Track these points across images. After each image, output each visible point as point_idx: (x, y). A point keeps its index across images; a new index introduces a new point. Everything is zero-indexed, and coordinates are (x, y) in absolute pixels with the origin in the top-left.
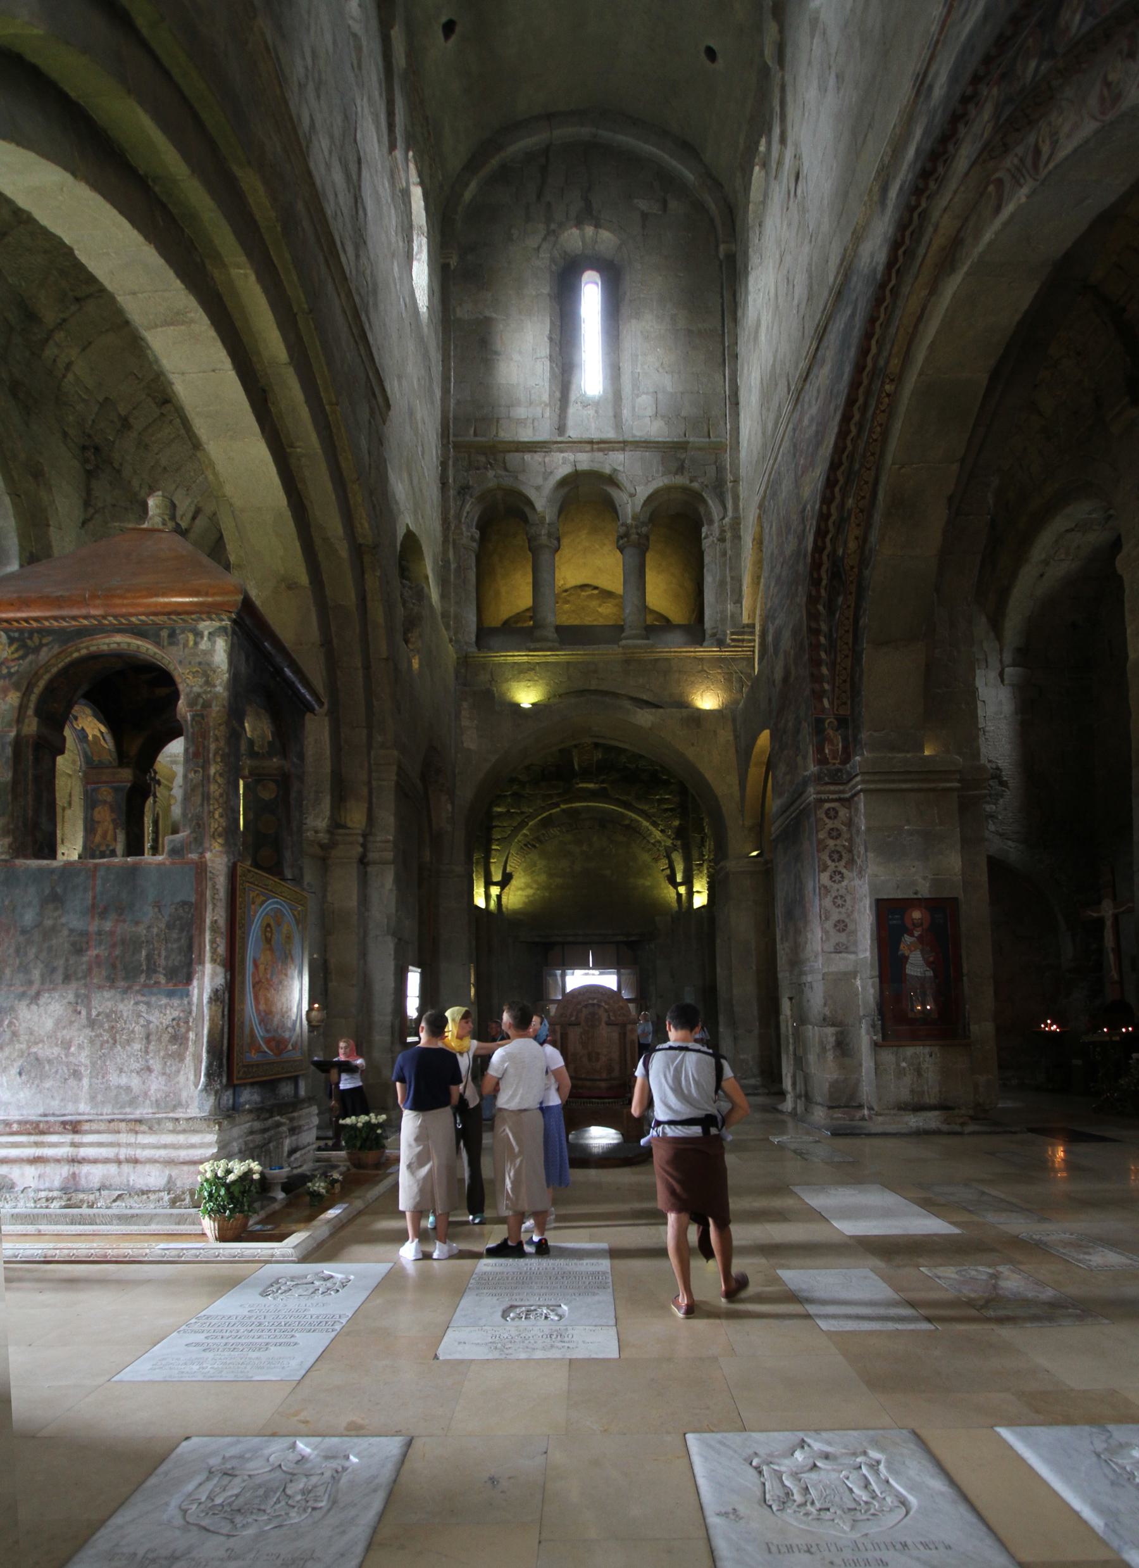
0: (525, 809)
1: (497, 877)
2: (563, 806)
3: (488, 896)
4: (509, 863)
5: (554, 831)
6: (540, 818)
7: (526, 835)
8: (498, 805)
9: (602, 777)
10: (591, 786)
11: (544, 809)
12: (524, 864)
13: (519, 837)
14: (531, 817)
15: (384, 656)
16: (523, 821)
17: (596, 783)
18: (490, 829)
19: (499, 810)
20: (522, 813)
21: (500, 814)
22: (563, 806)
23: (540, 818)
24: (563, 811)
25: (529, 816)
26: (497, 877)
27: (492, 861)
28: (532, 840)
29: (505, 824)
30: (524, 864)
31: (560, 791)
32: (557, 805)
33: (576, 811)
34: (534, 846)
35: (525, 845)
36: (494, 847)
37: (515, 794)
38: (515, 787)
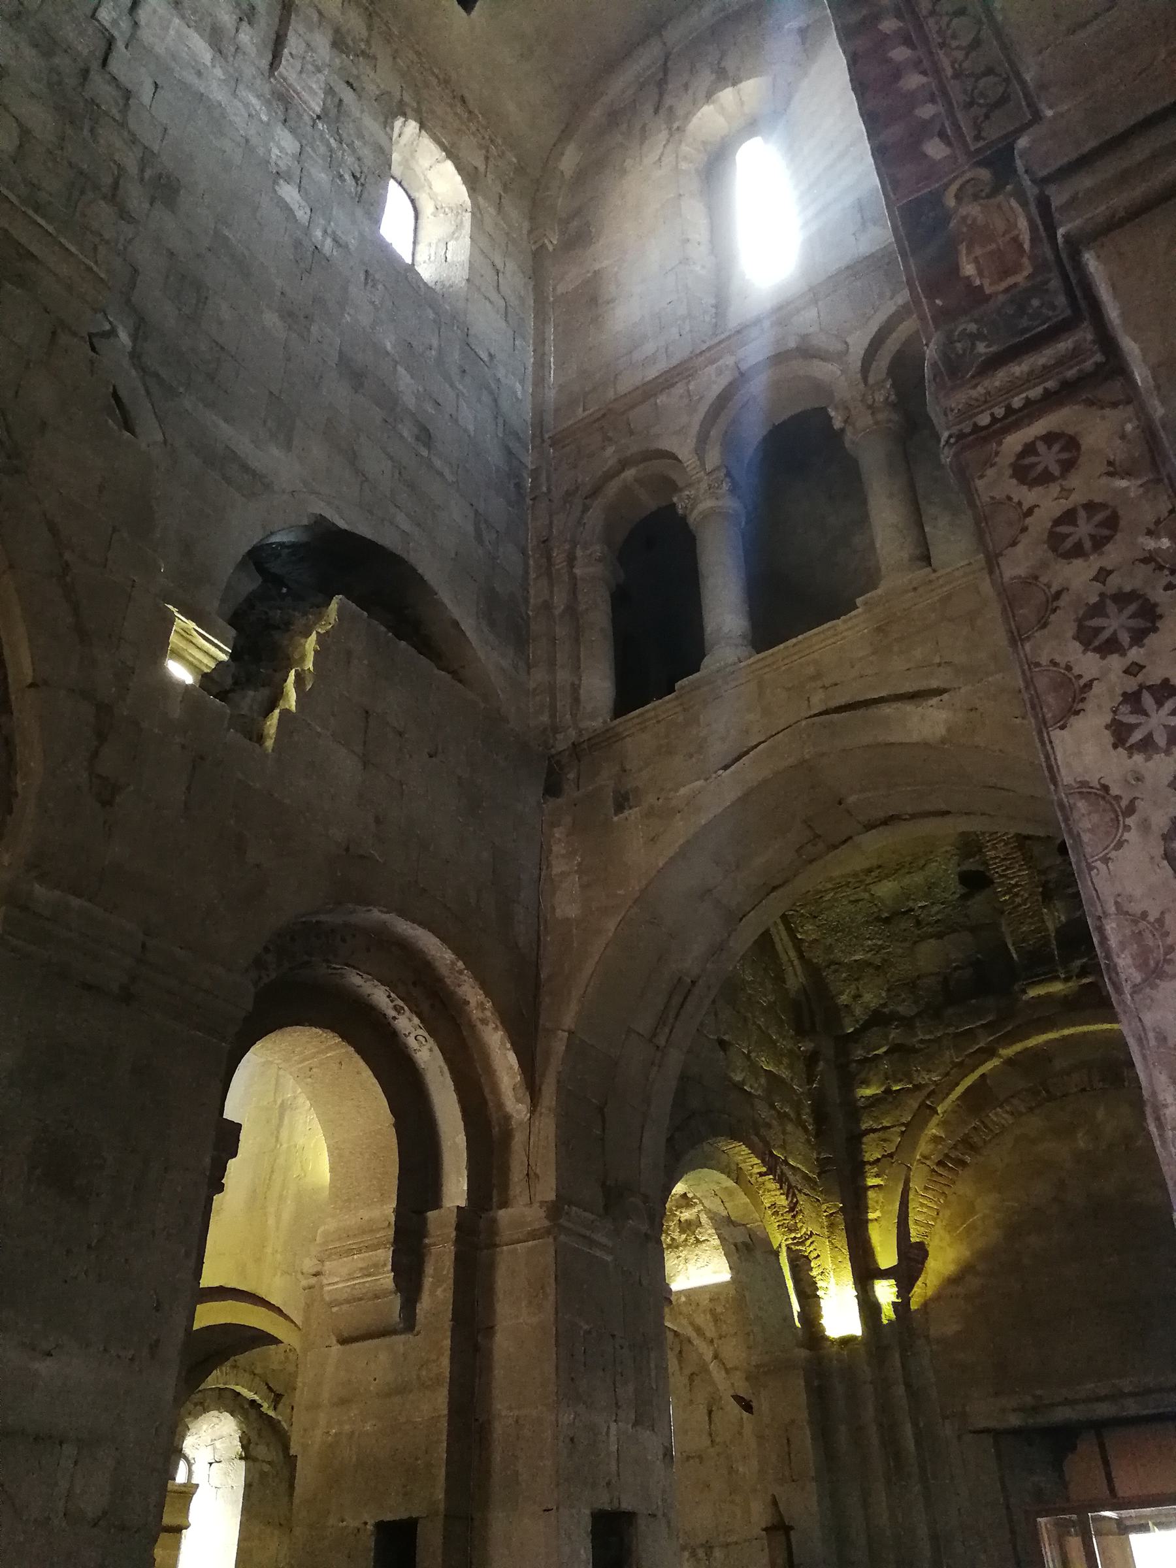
0: (923, 1078)
1: (886, 1256)
2: (1008, 1052)
3: (868, 1307)
4: (912, 1216)
5: (999, 1116)
6: (960, 1090)
7: (936, 1139)
8: (866, 1083)
9: (1079, 963)
10: (1057, 987)
11: (965, 1068)
12: (947, 1213)
13: (923, 1147)
14: (939, 1092)
15: (29, 680)
16: (923, 1105)
17: (1067, 980)
18: (855, 1140)
19: (868, 1092)
20: (918, 1087)
21: (874, 1101)
22: (1008, 1052)
23: (960, 1090)
24: (1010, 1062)
25: (929, 1096)
26: (886, 1256)
27: (871, 1216)
28: (955, 1147)
29: (886, 1123)
30: (947, 1213)
31: (991, 1018)
32: (990, 1052)
33: (1040, 1056)
34: (962, 1163)
35: (940, 1163)
36: (871, 1182)
37: (895, 1049)
38: (894, 1034)
